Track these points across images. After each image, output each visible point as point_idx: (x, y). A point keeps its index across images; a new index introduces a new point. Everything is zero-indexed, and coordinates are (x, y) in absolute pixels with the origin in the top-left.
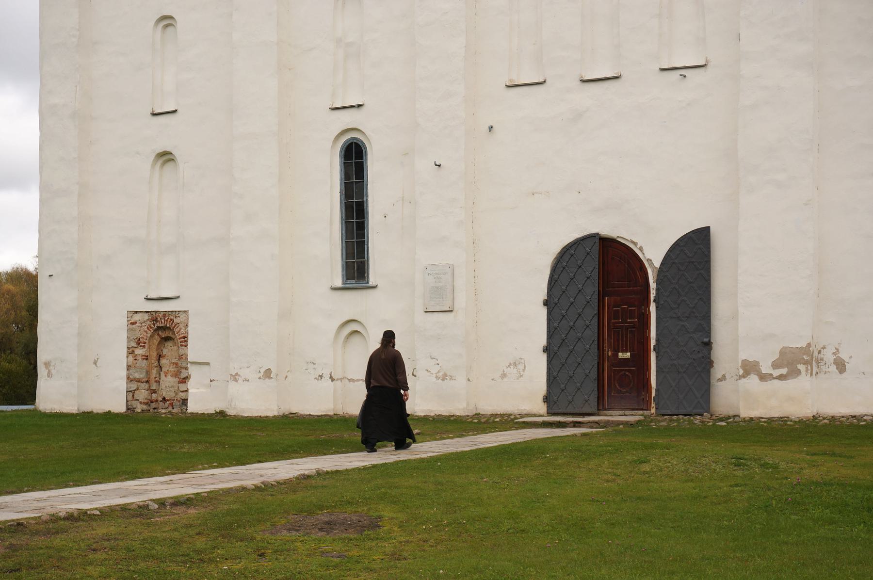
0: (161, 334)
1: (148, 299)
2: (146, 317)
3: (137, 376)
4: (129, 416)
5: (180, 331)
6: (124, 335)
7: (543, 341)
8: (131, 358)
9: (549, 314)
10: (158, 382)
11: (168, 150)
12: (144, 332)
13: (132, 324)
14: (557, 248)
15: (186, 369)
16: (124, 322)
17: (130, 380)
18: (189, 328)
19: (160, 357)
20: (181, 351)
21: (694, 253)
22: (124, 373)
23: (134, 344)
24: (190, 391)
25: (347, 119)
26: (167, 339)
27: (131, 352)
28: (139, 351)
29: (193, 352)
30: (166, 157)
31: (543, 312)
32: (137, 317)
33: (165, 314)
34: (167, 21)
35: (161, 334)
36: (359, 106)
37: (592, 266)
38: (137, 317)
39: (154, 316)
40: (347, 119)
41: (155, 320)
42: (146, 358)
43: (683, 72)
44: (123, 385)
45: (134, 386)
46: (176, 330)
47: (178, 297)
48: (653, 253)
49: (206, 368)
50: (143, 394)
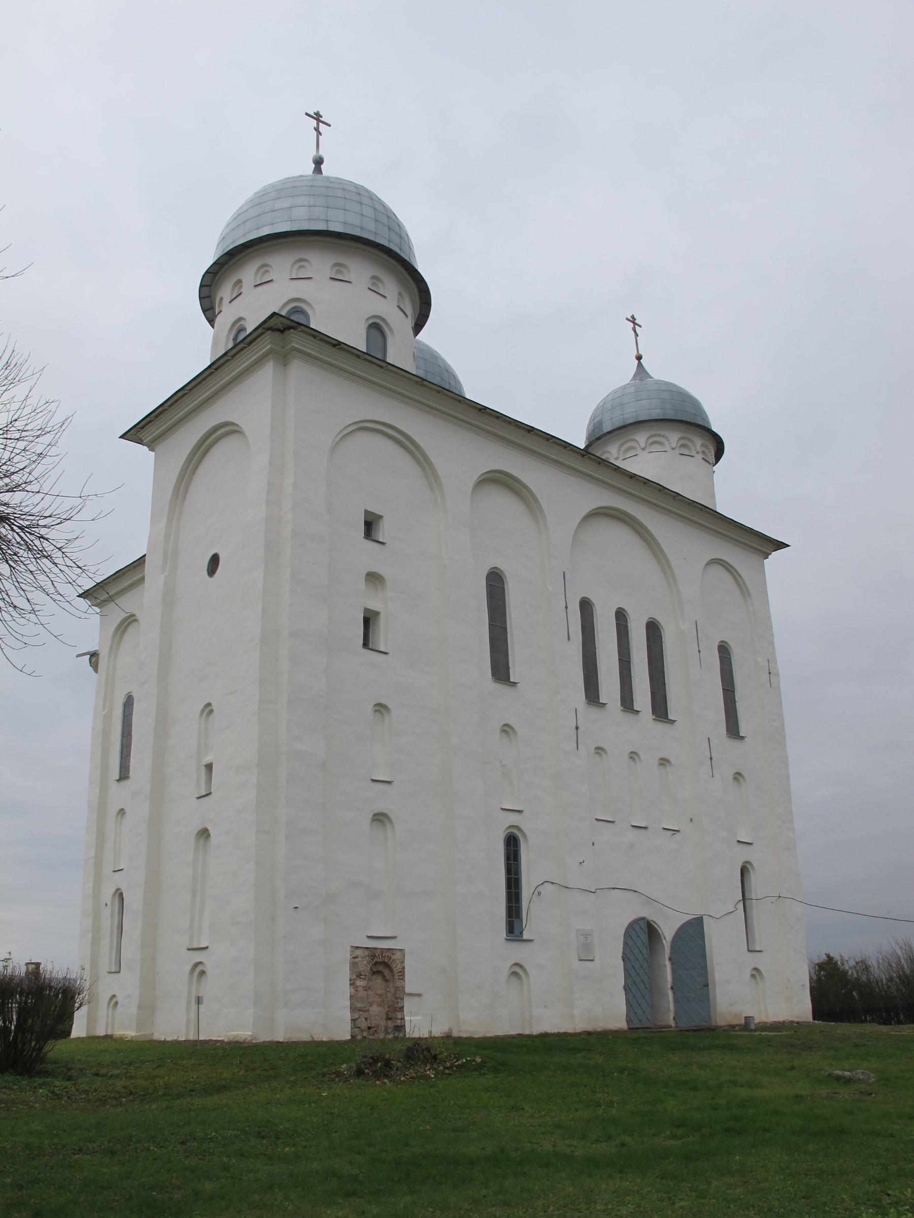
0: (380, 968)
2: (366, 953)
3: (359, 1005)
4: (640, 1035)
5: (396, 967)
7: (622, 982)
8: (353, 990)
11: (385, 811)
12: (364, 966)
13: (355, 958)
15: (402, 999)
16: (348, 956)
17: (353, 1009)
18: (406, 965)
20: (398, 984)
22: (348, 1003)
23: (355, 977)
24: (407, 1018)
25: (513, 819)
27: (352, 984)
28: (359, 983)
29: (410, 984)
30: (380, 818)
31: (621, 964)
32: (359, 952)
33: (383, 950)
34: (381, 708)
35: (380, 968)
36: (519, 811)
38: (359, 952)
39: (372, 953)
40: (513, 819)
41: (374, 956)
44: (347, 1015)
45: (356, 1016)
46: (393, 966)
47: (395, 938)
48: (668, 932)
49: (417, 999)
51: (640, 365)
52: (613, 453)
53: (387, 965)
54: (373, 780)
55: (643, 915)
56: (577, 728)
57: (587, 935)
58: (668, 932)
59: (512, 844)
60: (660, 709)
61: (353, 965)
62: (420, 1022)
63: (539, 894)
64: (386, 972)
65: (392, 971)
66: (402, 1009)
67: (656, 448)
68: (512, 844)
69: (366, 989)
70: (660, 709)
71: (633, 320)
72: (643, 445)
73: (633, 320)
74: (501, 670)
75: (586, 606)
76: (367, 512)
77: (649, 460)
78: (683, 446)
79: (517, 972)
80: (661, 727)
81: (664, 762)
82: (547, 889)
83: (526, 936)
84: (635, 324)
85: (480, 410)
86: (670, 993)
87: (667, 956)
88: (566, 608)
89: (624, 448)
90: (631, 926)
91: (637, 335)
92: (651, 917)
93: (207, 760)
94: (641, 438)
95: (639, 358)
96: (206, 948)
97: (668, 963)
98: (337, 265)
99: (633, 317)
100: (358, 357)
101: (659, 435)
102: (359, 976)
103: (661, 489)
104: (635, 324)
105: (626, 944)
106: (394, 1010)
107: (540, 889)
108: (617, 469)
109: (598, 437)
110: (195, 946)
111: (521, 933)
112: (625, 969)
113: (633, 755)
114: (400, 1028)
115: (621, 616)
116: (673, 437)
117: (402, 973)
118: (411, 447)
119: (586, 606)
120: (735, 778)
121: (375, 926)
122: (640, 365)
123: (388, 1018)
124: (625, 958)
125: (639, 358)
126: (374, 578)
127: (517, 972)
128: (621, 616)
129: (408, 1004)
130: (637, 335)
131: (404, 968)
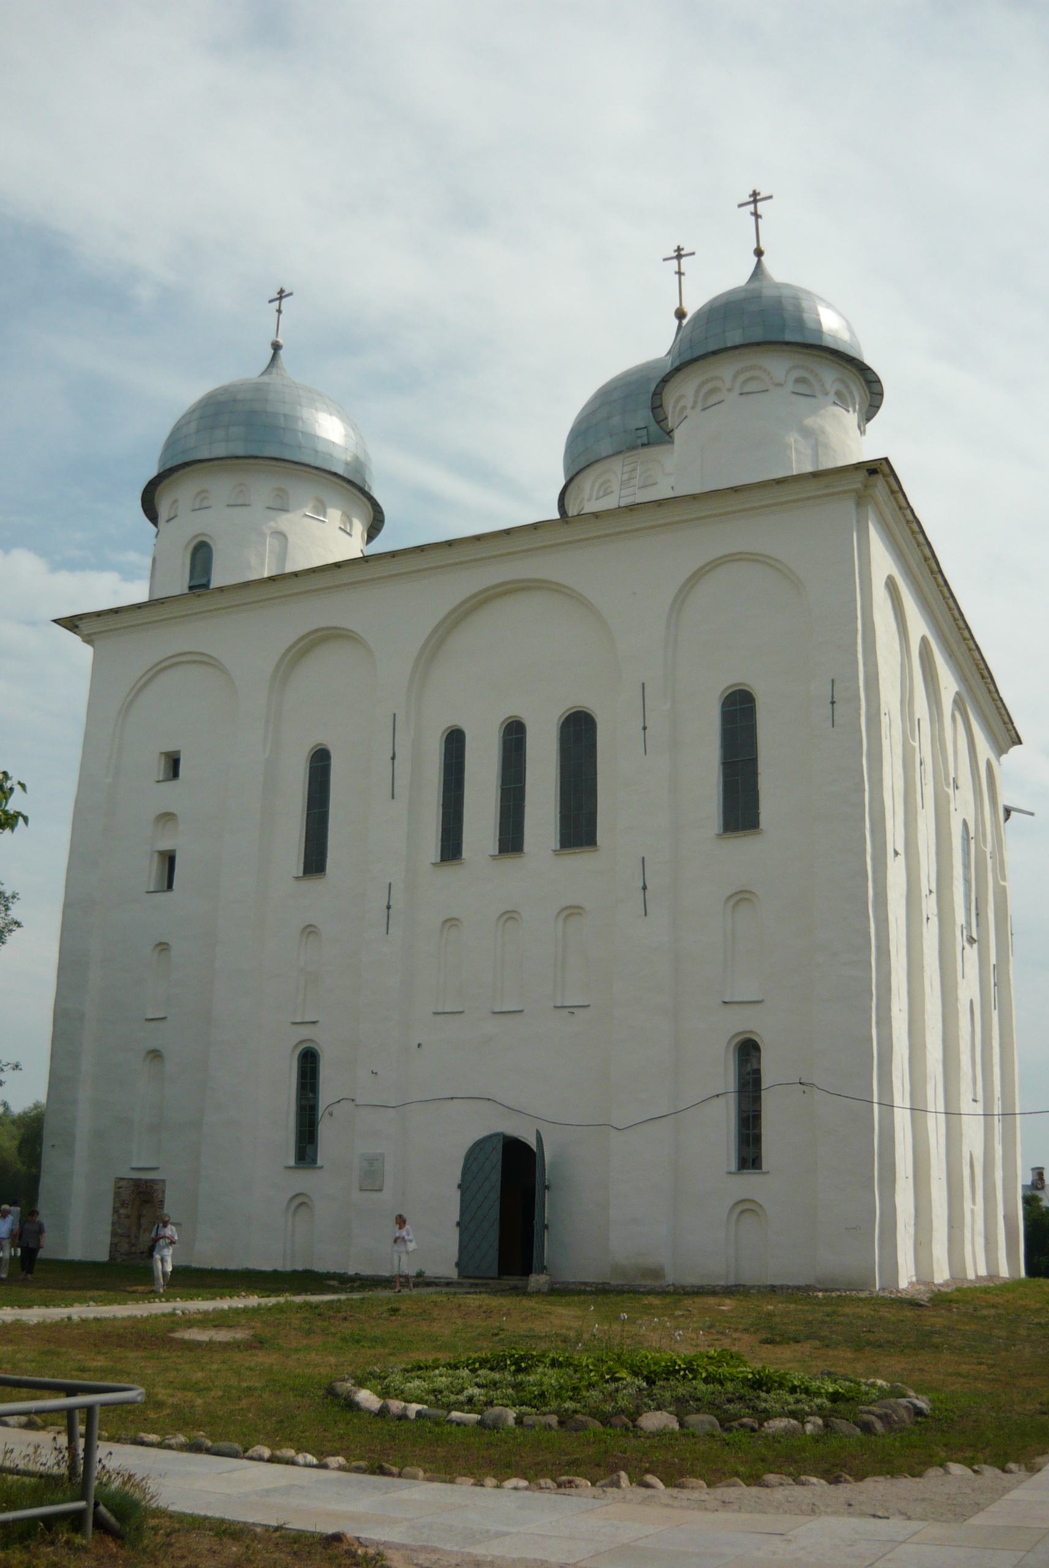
1: (133, 1169)
3: (119, 1231)
6: (111, 1196)
7: (457, 1219)
8: (116, 1217)
9: (462, 1195)
10: (137, 1237)
14: (470, 1143)
17: (114, 1234)
19: (140, 1216)
22: (109, 1228)
25: (304, 1032)
26: (146, 1202)
27: (116, 1211)
28: (122, 1211)
31: (457, 1194)
33: (147, 1181)
36: (314, 1023)
37: (497, 1157)
38: (122, 1183)
42: (128, 1217)
43: (571, 1010)
45: (116, 1240)
50: (124, 1247)
51: (759, 269)
55: (500, 1130)
61: (117, 1195)
63: (331, 1114)
79: (301, 1203)
81: (572, 911)
88: (393, 758)
90: (478, 1148)
95: (759, 253)
102: (123, 1204)
107: (330, 1109)
121: (138, 1158)
122: (759, 269)
125: (759, 253)
126: (167, 817)
127: (301, 1203)
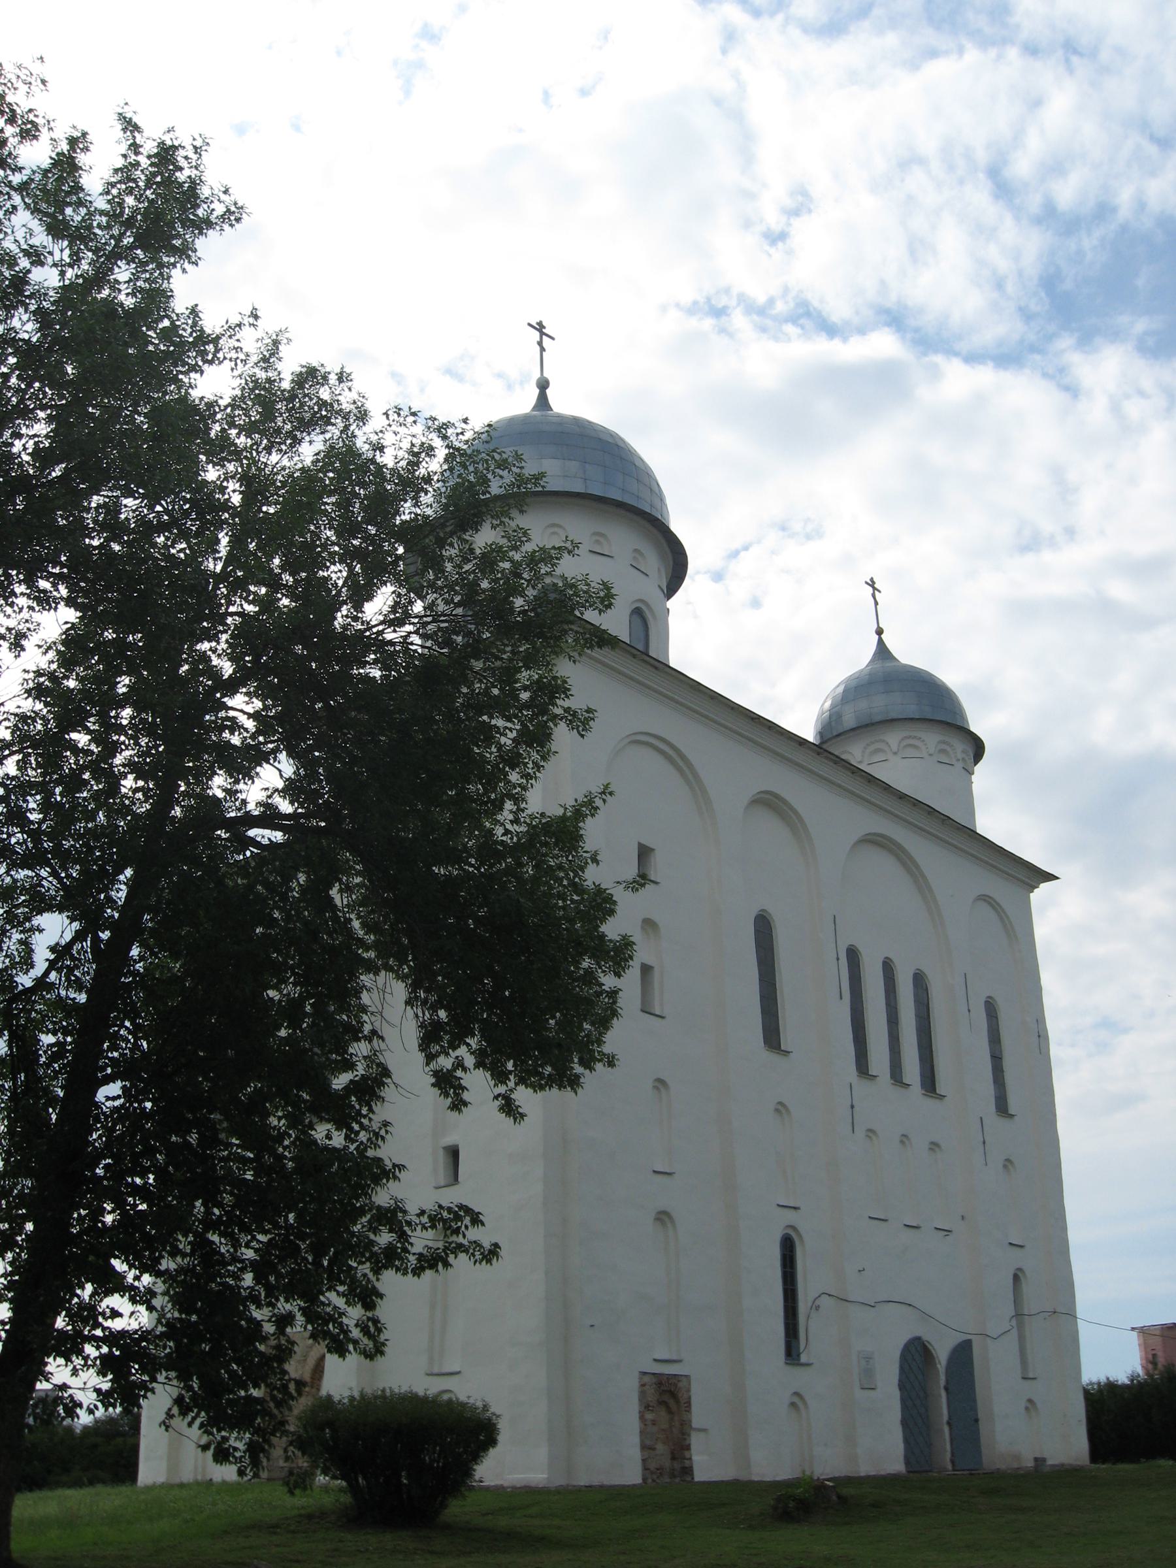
0: (666, 1397)
3: (648, 1442)
11: (668, 1210)
17: (644, 1447)
21: (963, 1353)
25: (790, 1217)
27: (642, 1418)
28: (649, 1416)
29: (698, 1416)
30: (663, 1217)
31: (897, 1393)
32: (646, 1379)
35: (666, 1397)
38: (646, 1379)
40: (790, 1217)
48: (942, 1354)
49: (702, 1435)
51: (881, 642)
52: (855, 753)
53: (673, 1395)
54: (655, 1172)
56: (852, 1107)
57: (868, 1358)
58: (942, 1354)
59: (788, 1249)
60: (929, 1084)
61: (642, 1394)
62: (709, 1463)
63: (817, 1308)
64: (672, 1403)
65: (677, 1402)
66: (688, 1448)
67: (910, 752)
68: (788, 1249)
69: (654, 1423)
70: (929, 1084)
71: (872, 584)
72: (895, 749)
73: (872, 584)
74: (772, 1037)
75: (853, 955)
76: (639, 844)
77: (900, 765)
78: (942, 751)
79: (797, 1403)
80: (930, 1103)
81: (934, 1146)
82: (825, 1302)
83: (804, 1358)
84: (874, 589)
85: (753, 719)
86: (946, 1429)
87: (942, 1382)
89: (872, 748)
91: (876, 603)
92: (926, 1337)
93: (449, 1140)
94: (893, 738)
95: (879, 632)
96: (459, 1373)
97: (943, 1393)
98: (595, 534)
99: (872, 580)
100: (634, 656)
101: (915, 737)
103: (931, 811)
104: (874, 589)
105: (902, 1369)
106: (680, 1449)
107: (817, 1303)
108: (855, 771)
109: (834, 729)
110: (436, 1370)
111: (799, 1355)
112: (903, 1400)
113: (904, 1139)
114: (688, 1471)
115: (888, 968)
116: (931, 739)
117: (689, 1403)
118: (681, 763)
119: (853, 955)
120: (1005, 1166)
122: (881, 642)
123: (673, 1458)
124: (902, 1386)
125: (879, 632)
127: (797, 1403)
128: (888, 968)
129: (696, 1441)
130: (876, 603)
131: (690, 1398)
